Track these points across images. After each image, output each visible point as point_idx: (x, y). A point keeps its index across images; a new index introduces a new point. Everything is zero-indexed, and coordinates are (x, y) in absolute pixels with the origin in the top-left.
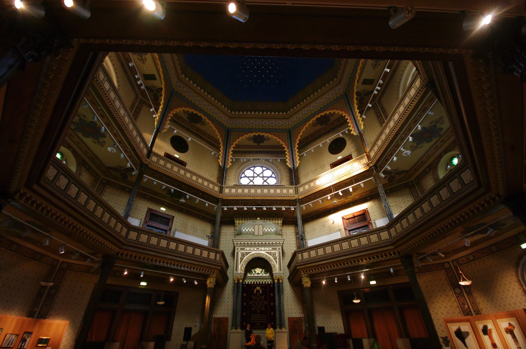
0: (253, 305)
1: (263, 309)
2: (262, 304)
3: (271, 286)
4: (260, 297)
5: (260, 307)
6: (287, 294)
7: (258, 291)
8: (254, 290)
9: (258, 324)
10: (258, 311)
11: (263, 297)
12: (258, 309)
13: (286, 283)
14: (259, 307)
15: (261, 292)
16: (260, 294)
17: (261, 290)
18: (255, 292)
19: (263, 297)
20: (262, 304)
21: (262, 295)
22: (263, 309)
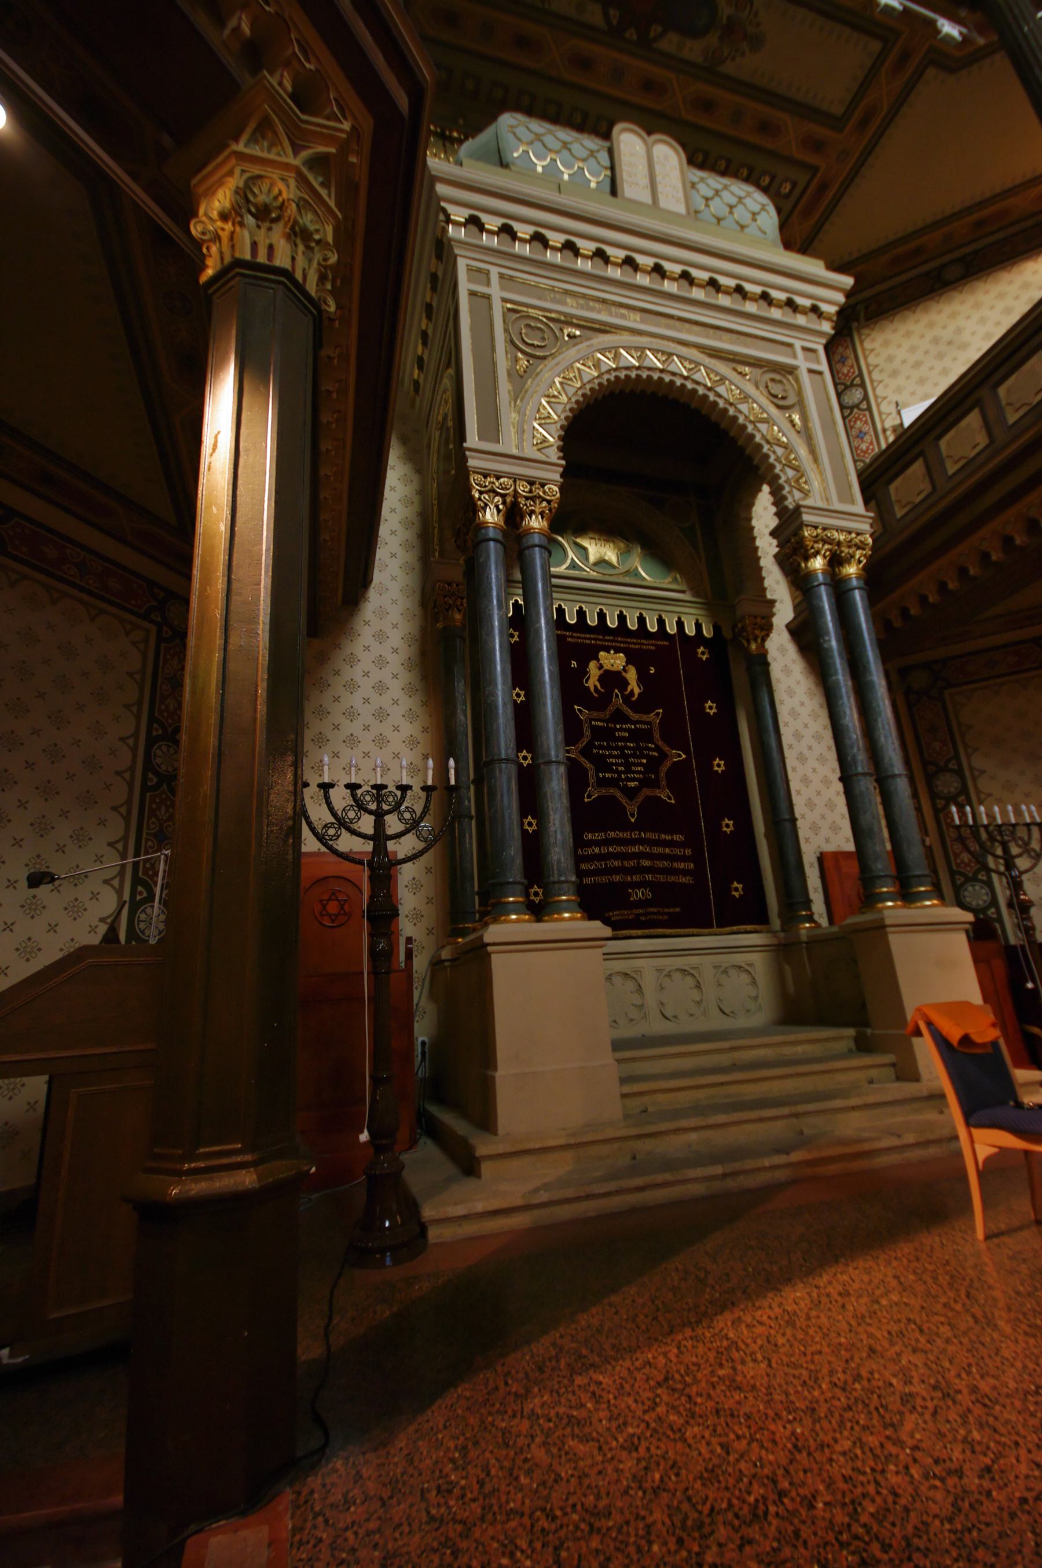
0: (588, 765)
1: (664, 794)
2: (653, 765)
3: (702, 653)
4: (635, 716)
5: (645, 783)
6: (794, 714)
7: (612, 679)
8: (583, 671)
9: (639, 894)
10: (632, 809)
11: (655, 717)
12: (630, 794)
13: (782, 650)
14: (632, 784)
15: (634, 687)
16: (627, 698)
17: (632, 675)
18: (593, 681)
19: (655, 717)
20: (653, 765)
21: (643, 705)
22: (664, 794)
